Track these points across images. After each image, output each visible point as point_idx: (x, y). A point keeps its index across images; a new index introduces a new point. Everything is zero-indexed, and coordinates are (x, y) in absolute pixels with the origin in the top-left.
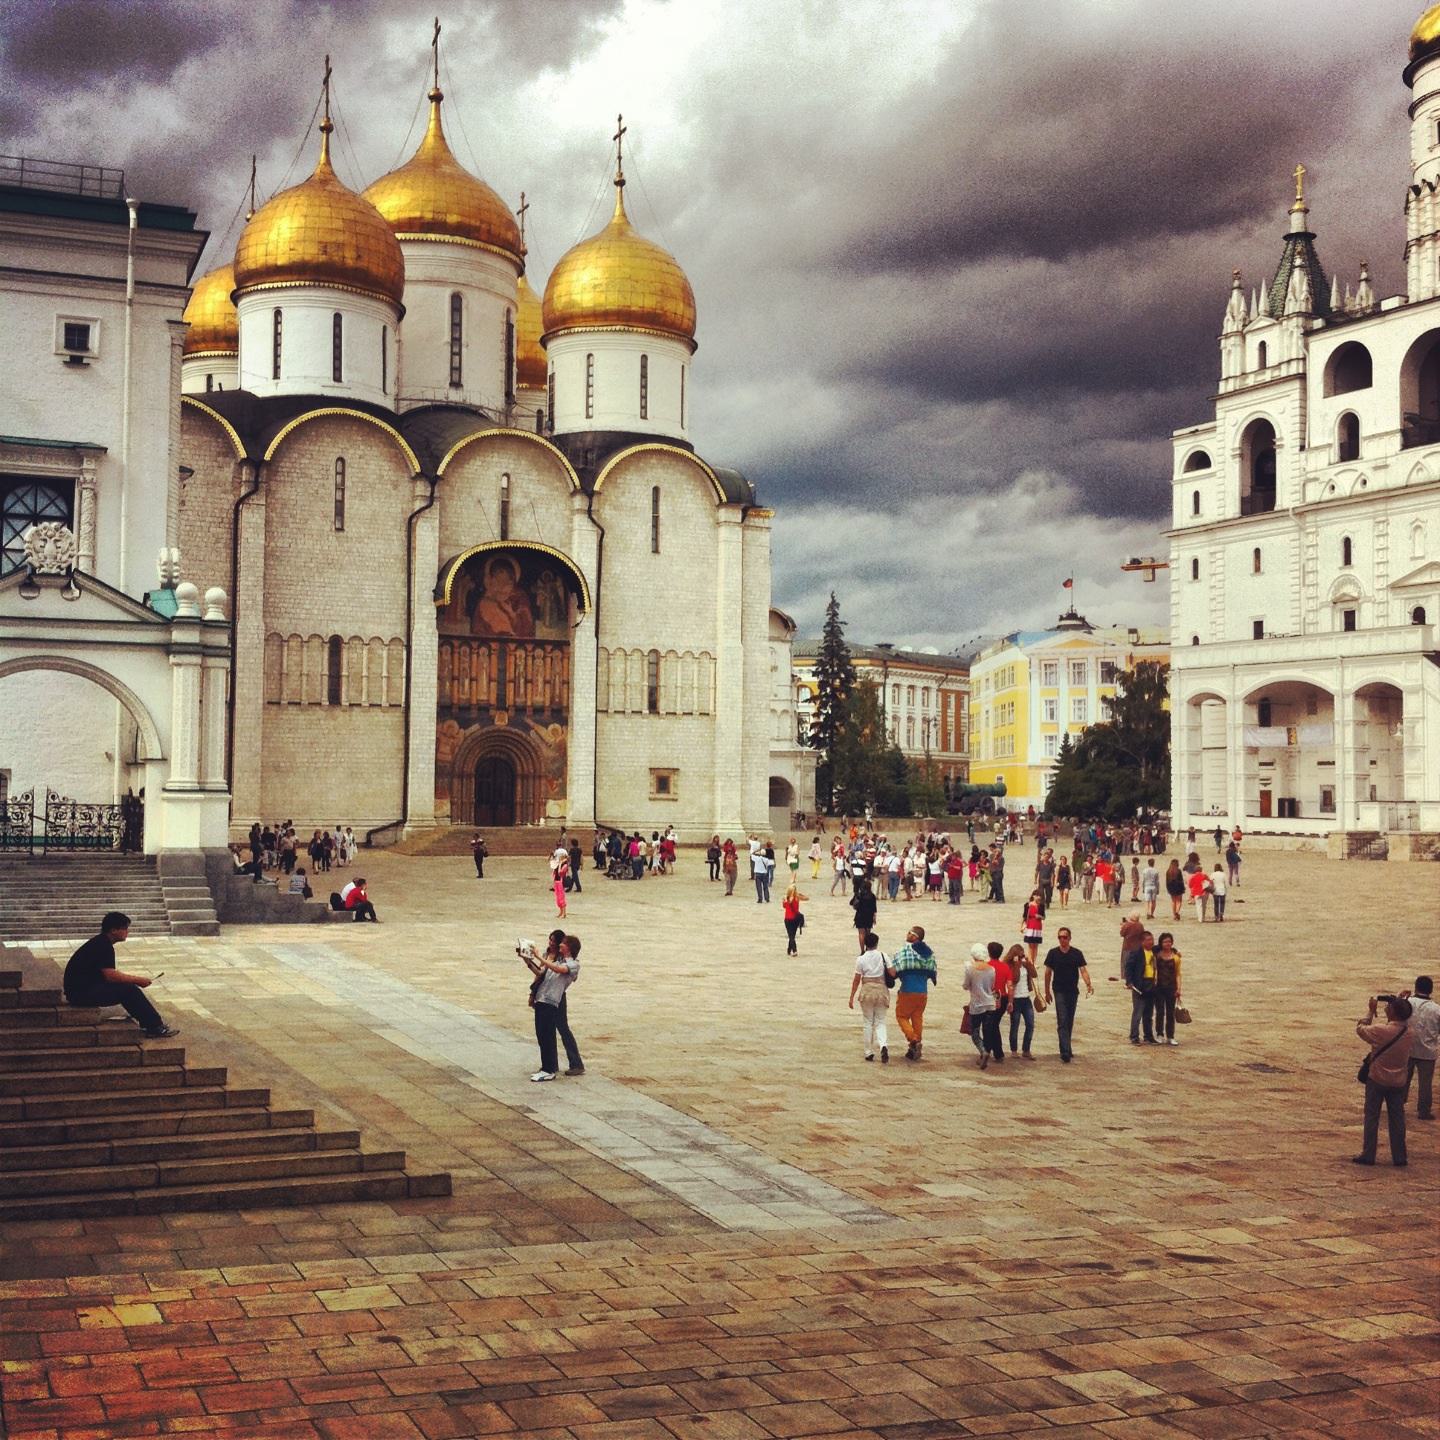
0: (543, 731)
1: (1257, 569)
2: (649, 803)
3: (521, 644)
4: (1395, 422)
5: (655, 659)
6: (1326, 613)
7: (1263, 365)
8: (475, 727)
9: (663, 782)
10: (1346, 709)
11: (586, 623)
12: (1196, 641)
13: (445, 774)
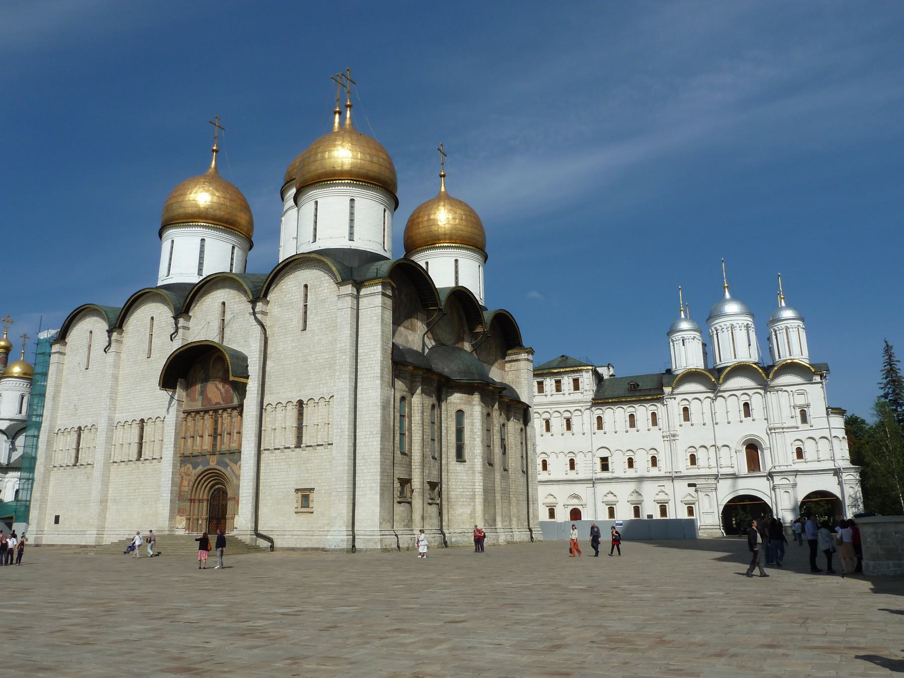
2: (295, 515)
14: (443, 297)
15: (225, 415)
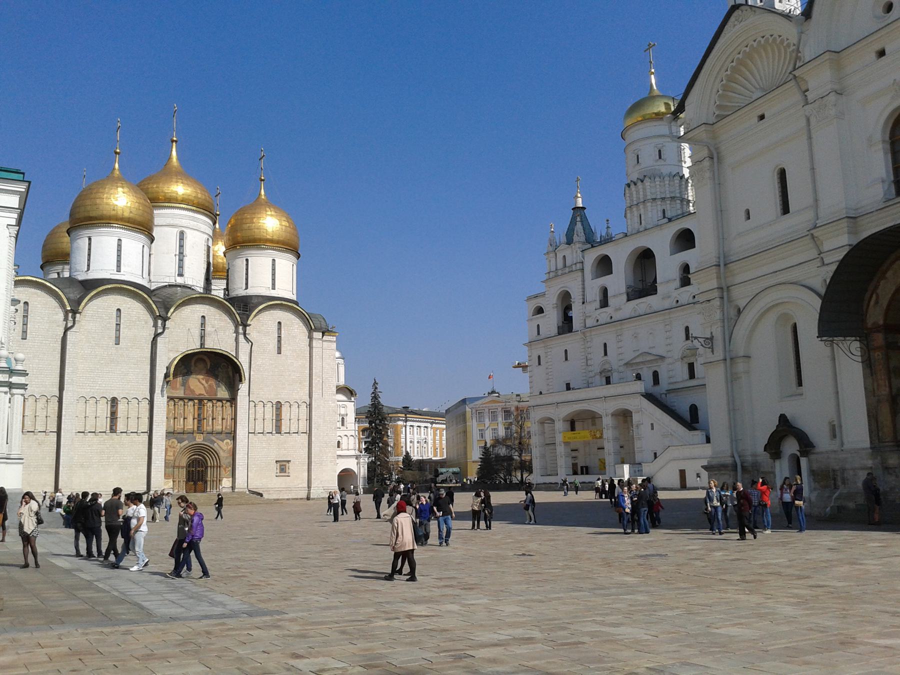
0: (220, 443)
1: (566, 359)
3: (209, 400)
4: (623, 289)
5: (279, 406)
6: (598, 377)
7: (565, 266)
8: (186, 442)
9: (283, 467)
10: (607, 421)
11: (243, 388)
12: (541, 393)
13: (170, 467)
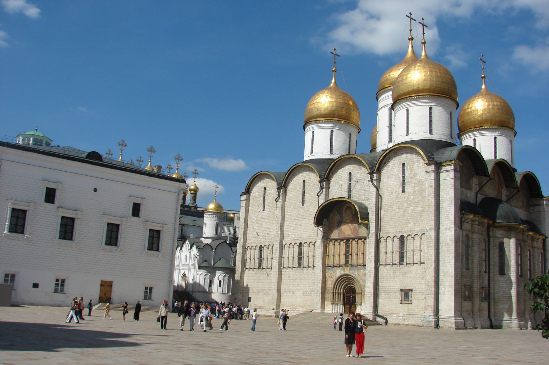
9: (406, 295)
14: (490, 167)
15: (354, 243)
